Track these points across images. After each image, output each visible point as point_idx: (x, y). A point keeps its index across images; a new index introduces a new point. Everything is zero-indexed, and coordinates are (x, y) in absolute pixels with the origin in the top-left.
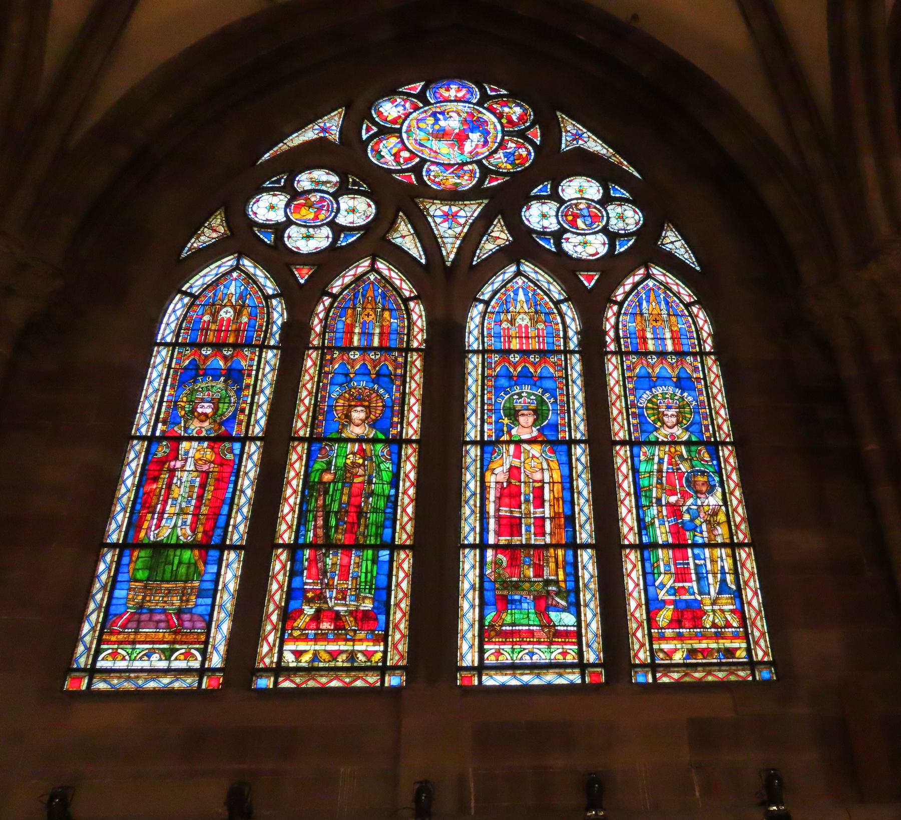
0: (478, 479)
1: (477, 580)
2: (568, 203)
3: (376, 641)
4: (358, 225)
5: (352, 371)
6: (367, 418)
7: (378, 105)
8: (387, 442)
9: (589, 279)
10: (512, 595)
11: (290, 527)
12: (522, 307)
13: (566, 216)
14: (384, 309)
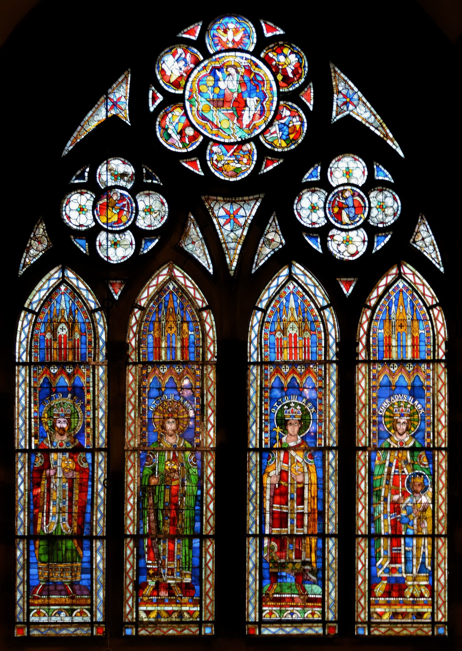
0: (258, 481)
1: (258, 560)
2: (336, 191)
3: (195, 603)
4: (155, 228)
5: (163, 385)
6: (178, 428)
7: (161, 59)
8: (193, 451)
9: (348, 284)
10: (280, 573)
11: (133, 522)
12: (292, 314)
13: (333, 207)
14: (183, 322)
